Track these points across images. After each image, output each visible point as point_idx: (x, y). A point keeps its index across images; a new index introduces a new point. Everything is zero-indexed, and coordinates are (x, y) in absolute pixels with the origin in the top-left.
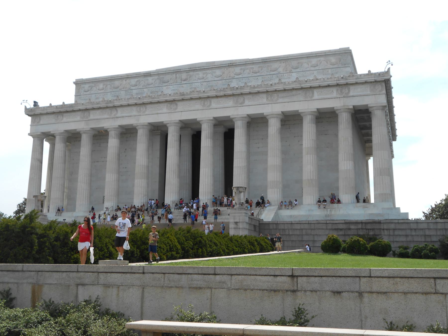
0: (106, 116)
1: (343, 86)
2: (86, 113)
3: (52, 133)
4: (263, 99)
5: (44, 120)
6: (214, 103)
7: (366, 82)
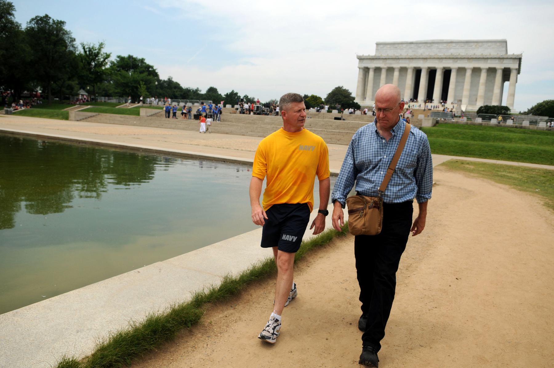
1: (501, 59)
5: (365, 61)
6: (444, 61)
7: (511, 58)
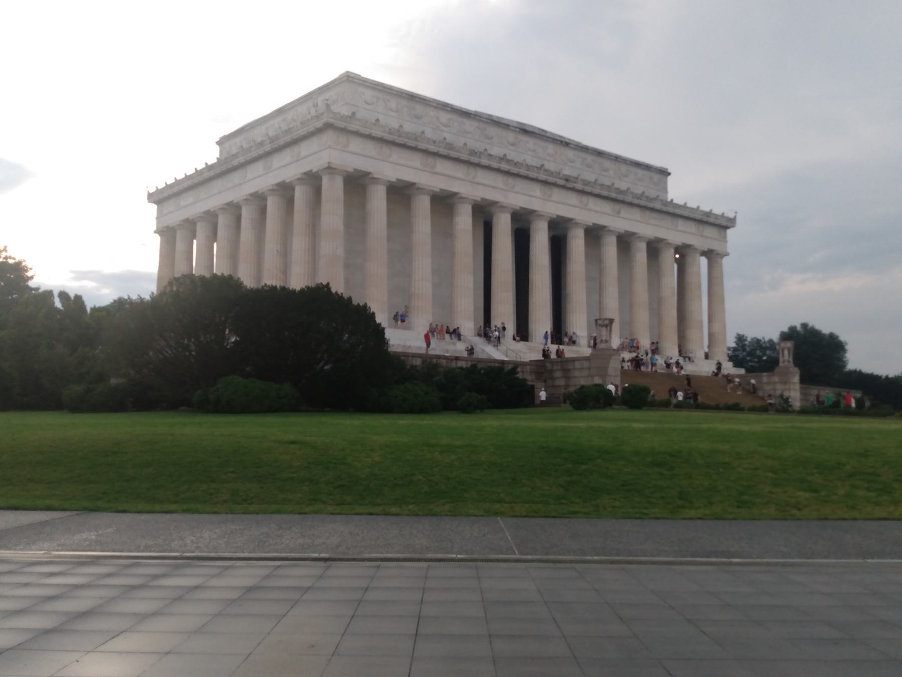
0: (460, 175)
2: (430, 160)
3: (375, 176)
4: (636, 214)
6: (593, 203)
